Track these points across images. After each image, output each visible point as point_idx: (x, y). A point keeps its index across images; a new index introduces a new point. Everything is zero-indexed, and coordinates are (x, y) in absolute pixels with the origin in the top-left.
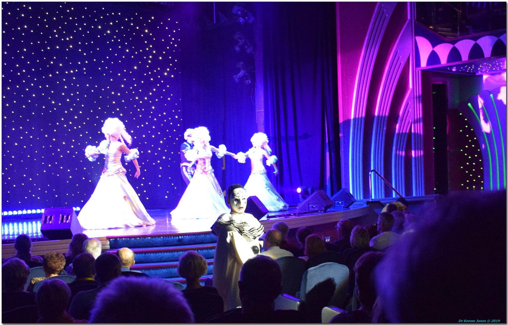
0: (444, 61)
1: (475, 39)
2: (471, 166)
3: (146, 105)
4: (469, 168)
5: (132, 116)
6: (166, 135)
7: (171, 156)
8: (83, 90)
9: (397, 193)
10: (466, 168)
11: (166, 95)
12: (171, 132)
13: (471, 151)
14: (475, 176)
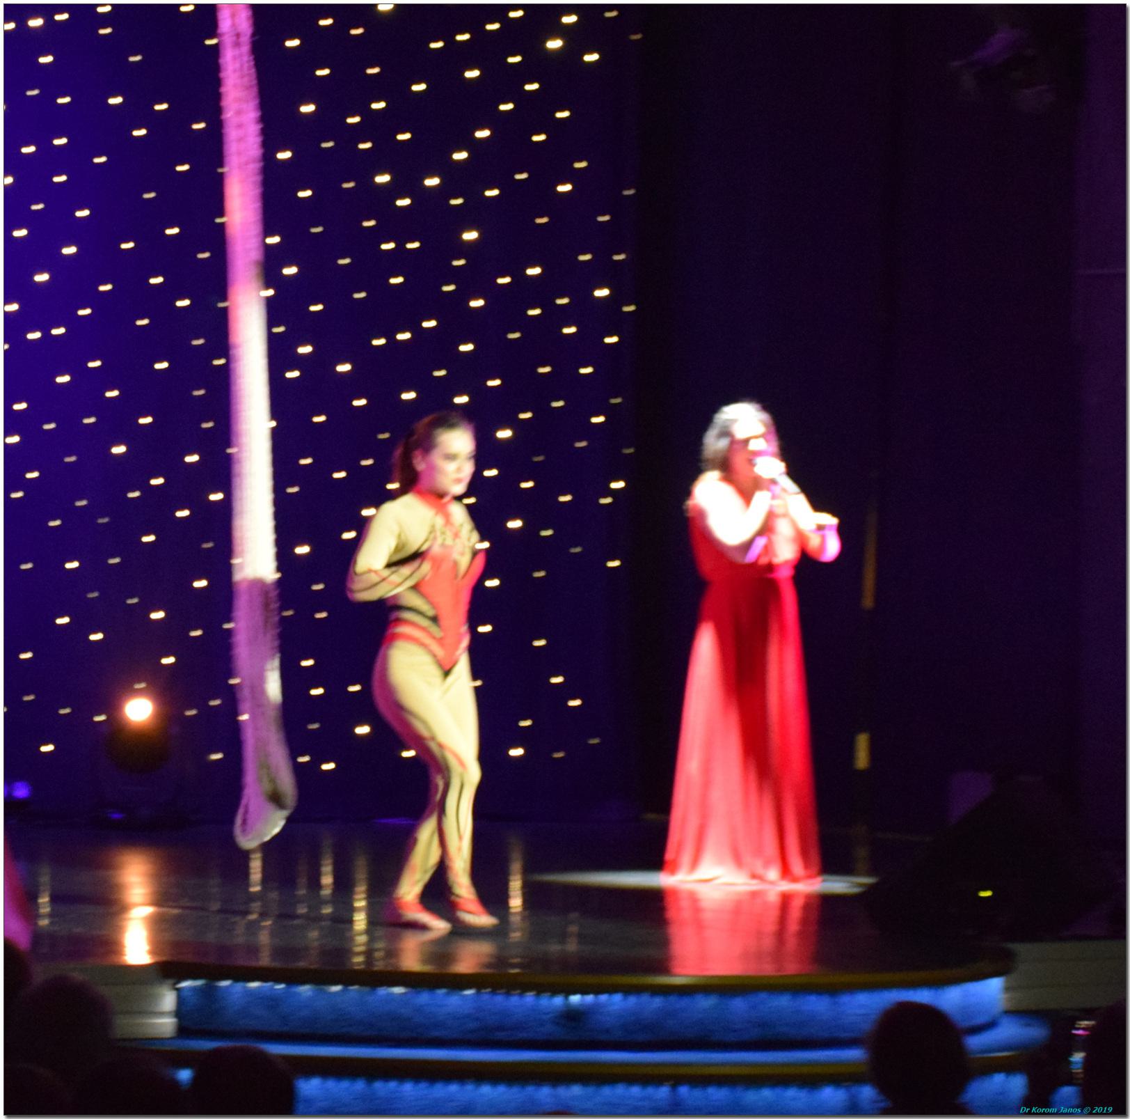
3: (433, 220)
5: (352, 278)
6: (537, 394)
7: (557, 515)
8: (93, 126)
11: (550, 165)
12: (564, 381)
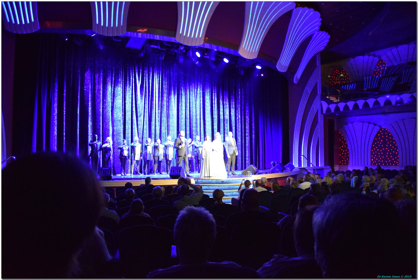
0: (333, 111)
1: (346, 102)
2: (344, 155)
4: (344, 155)
9: (313, 165)
10: (342, 155)
13: (344, 149)
14: (346, 159)
